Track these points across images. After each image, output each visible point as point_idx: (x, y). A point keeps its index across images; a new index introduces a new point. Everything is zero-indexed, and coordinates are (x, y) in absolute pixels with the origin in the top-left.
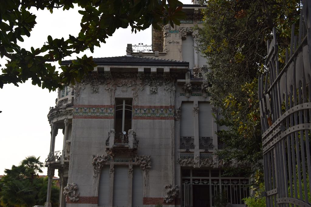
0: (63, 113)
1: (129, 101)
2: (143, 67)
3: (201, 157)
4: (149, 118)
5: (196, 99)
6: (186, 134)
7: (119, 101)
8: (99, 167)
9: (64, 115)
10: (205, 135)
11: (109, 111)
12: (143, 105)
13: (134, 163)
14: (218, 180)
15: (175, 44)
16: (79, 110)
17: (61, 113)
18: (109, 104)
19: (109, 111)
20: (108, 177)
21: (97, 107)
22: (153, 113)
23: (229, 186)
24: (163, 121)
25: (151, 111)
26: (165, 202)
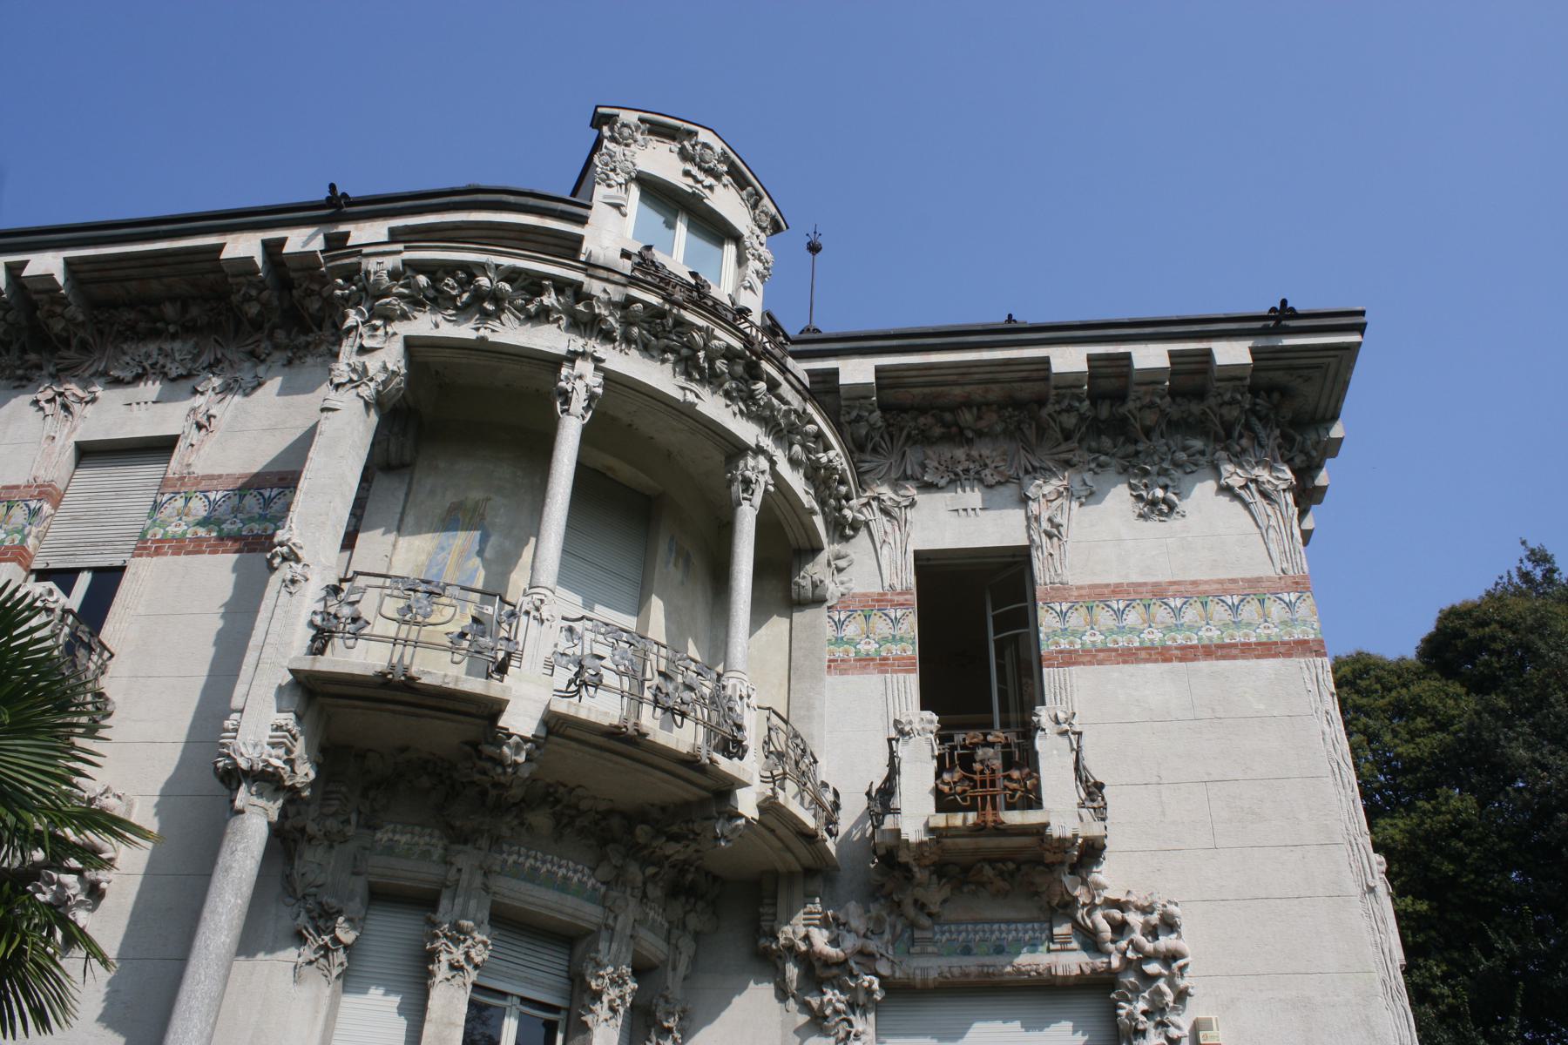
0: (775, 401)
17: (762, 386)
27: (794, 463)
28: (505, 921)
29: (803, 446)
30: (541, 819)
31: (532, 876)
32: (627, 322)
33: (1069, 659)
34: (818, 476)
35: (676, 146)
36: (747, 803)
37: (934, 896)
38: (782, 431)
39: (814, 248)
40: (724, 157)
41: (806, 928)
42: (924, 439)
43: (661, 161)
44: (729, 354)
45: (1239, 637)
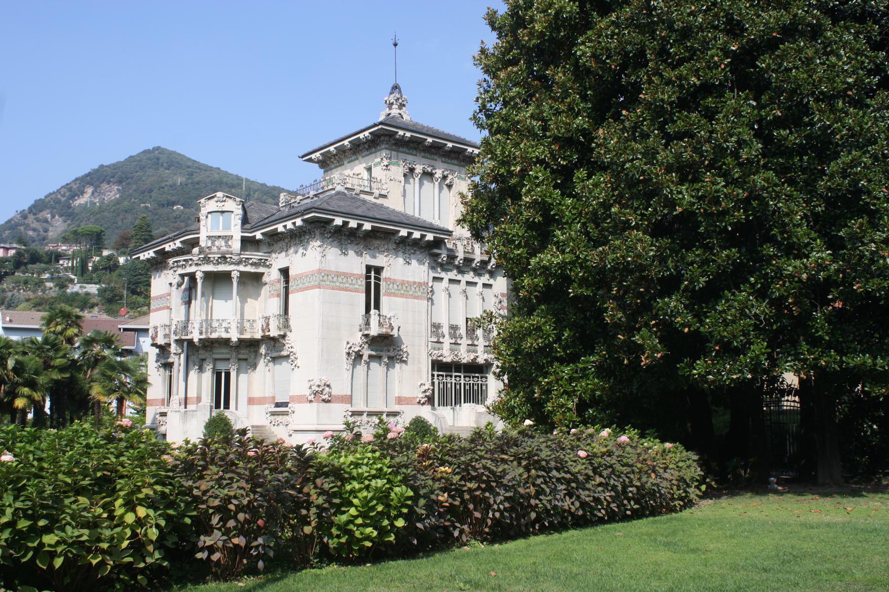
1: (378, 270)
2: (407, 230)
3: (452, 350)
4: (402, 296)
5: (446, 276)
6: (436, 320)
7: (369, 268)
9: (232, 263)
10: (454, 323)
11: (359, 282)
14: (460, 377)
16: (325, 278)
19: (359, 282)
20: (361, 369)
21: (346, 275)
22: (406, 289)
24: (416, 301)
25: (404, 288)
26: (419, 403)
27: (245, 266)
30: (216, 345)
34: (253, 264)
36: (234, 339)
37: (272, 343)
38: (239, 263)
39: (395, 45)
41: (263, 350)
42: (277, 241)
45: (310, 285)
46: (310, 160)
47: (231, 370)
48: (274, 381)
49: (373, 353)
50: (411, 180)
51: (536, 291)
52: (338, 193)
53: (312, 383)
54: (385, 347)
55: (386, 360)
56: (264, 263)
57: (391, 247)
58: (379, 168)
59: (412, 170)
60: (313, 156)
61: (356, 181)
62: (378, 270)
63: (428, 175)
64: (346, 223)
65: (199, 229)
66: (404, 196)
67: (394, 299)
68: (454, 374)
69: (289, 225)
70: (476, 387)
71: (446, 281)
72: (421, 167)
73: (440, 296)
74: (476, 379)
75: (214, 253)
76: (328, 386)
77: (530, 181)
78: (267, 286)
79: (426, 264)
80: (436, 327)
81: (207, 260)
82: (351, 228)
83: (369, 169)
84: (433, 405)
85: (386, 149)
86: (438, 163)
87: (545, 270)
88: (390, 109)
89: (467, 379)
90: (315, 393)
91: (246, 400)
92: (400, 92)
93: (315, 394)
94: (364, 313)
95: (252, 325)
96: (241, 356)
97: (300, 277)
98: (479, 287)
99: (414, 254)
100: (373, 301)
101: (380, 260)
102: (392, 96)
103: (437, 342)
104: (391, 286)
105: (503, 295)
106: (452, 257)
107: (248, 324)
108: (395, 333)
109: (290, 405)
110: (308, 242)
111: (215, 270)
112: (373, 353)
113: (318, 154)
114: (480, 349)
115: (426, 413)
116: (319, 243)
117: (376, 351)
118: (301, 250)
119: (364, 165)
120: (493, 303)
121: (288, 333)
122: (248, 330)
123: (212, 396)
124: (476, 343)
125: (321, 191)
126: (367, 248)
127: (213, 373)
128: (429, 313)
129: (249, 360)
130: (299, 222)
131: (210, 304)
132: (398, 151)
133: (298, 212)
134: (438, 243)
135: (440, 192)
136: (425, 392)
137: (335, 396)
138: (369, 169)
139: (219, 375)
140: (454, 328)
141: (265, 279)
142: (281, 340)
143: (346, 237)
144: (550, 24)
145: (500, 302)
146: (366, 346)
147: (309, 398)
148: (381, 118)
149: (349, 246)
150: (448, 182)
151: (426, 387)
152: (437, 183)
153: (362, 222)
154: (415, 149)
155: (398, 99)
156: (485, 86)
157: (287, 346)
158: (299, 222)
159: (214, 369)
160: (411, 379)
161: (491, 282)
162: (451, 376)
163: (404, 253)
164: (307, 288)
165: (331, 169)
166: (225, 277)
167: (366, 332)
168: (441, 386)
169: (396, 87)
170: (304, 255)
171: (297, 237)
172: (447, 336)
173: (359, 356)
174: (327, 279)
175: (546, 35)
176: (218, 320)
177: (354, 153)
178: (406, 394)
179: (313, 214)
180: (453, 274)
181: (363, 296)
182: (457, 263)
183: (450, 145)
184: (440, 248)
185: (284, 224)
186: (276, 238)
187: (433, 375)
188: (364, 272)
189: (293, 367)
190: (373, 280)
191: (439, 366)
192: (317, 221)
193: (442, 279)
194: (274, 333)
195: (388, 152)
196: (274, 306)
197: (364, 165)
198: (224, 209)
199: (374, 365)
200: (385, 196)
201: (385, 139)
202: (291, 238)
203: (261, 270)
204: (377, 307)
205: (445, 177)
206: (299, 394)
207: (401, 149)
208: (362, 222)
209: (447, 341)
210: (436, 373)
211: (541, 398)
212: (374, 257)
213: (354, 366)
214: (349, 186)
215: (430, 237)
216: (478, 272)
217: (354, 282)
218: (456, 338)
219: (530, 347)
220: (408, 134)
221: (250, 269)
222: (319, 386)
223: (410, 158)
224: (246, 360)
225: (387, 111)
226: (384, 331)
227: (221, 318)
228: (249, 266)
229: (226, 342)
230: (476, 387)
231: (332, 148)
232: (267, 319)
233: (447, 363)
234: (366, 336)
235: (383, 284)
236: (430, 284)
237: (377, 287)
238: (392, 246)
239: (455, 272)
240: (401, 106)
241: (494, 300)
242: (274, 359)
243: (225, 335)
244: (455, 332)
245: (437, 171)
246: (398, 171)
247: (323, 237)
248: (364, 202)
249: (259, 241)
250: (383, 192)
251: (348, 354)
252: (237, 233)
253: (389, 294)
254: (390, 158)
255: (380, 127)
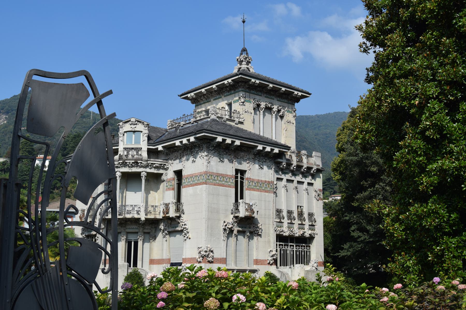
1: (243, 172)
2: (262, 146)
4: (258, 190)
6: (279, 208)
7: (237, 171)
8: (227, 232)
9: (142, 167)
11: (231, 181)
12: (254, 178)
13: (250, 229)
14: (293, 246)
15: (249, 114)
16: (210, 177)
17: (140, 164)
18: (231, 174)
19: (231, 181)
21: (223, 176)
22: (261, 186)
23: (284, 250)
24: (267, 194)
26: (269, 263)
28: (128, 233)
29: (150, 166)
30: (129, 223)
31: (130, 229)
32: (121, 165)
33: (185, 187)
34: (156, 168)
35: (128, 123)
36: (143, 219)
37: (169, 222)
39: (244, 22)
40: (136, 121)
41: (162, 227)
42: (173, 152)
43: (127, 127)
44: (133, 163)
46: (187, 98)
47: (139, 240)
48: (169, 248)
49: (240, 229)
50: (258, 112)
51: (431, 186)
52: (213, 120)
53: (201, 249)
54: (247, 226)
55: (248, 234)
56: (163, 167)
57: (251, 157)
58: (237, 104)
59: (259, 106)
60: (189, 95)
61: (223, 113)
62: (243, 172)
63: (269, 109)
64: (224, 140)
65: (118, 143)
66: (254, 123)
67: (253, 192)
68: (290, 244)
69: (185, 141)
70: (303, 253)
71: (285, 180)
72: (265, 104)
73: (282, 192)
74: (303, 248)
75: (130, 160)
76: (212, 251)
77: (429, 111)
78: (165, 183)
79: (273, 169)
80: (279, 212)
81: (124, 164)
82: (228, 144)
83: (230, 105)
84: (277, 266)
85: (242, 91)
86: (275, 101)
87: (442, 172)
88: (241, 64)
89: (298, 247)
90: (203, 257)
91: (148, 261)
92: (247, 54)
93: (203, 257)
94: (234, 202)
95: (155, 209)
96: (146, 231)
97: (191, 176)
98: (305, 186)
99: (265, 162)
100: (239, 194)
101: (244, 166)
102: (242, 56)
103: (279, 222)
104: (251, 183)
105: (320, 190)
106: (289, 164)
107: (152, 209)
108: (255, 215)
109: (183, 265)
110: (197, 153)
111: (130, 171)
112: (240, 229)
113: (192, 94)
114: (307, 227)
115: (273, 270)
116: (206, 154)
117: (242, 228)
118: (191, 159)
119: (226, 102)
120: (314, 196)
121: (182, 215)
122: (153, 213)
123: (125, 258)
124: (304, 223)
125: (198, 119)
126: (236, 157)
127: (126, 242)
128: (275, 202)
129: (151, 233)
130: (192, 139)
131: (124, 195)
132: (250, 93)
133: (193, 132)
134: (281, 155)
135: (276, 121)
136: (273, 256)
137: (216, 259)
138: (230, 105)
139: (129, 244)
140: (290, 213)
141: (163, 177)
142: (177, 220)
143: (223, 151)
144: (439, 5)
145: (319, 195)
146: (236, 225)
147: (199, 260)
148: (236, 71)
149: (225, 156)
150: (281, 114)
151: (274, 252)
152: (274, 115)
153: (234, 140)
154: (261, 91)
155: (246, 58)
156: (364, 47)
157: (181, 224)
158: (192, 139)
159: (126, 239)
160: (264, 247)
161: (313, 181)
162: (288, 246)
163: (259, 161)
164: (197, 184)
165: (201, 104)
166: (138, 175)
167: (236, 215)
168: (282, 252)
169: (244, 50)
170: (194, 161)
171: (189, 150)
172: (286, 218)
173: (231, 231)
174: (210, 178)
175: (435, 12)
176: (132, 206)
177: (219, 94)
178: (261, 257)
179: (203, 134)
180: (289, 176)
181: (233, 190)
182: (292, 168)
183: (283, 89)
184: (282, 158)
185: (180, 140)
186: (172, 150)
187: (277, 245)
188: (234, 174)
189: (185, 238)
190: (239, 179)
191: (280, 238)
192: (205, 139)
193: (282, 179)
194: (172, 214)
195: (244, 93)
196: (170, 197)
197: (226, 102)
198: (136, 129)
199: (240, 237)
200: (242, 123)
201: (244, 84)
202: (185, 150)
203: (161, 171)
204: (242, 198)
205: (279, 111)
206: (190, 257)
207: (252, 91)
208: (234, 140)
209: (286, 221)
210: (278, 243)
211: (433, 261)
212: (240, 163)
213: (228, 239)
214: (219, 115)
215: (276, 150)
216: (305, 175)
217: (228, 180)
218: (291, 219)
219: (430, 225)
220: (258, 82)
221: (153, 171)
222: (206, 252)
223: (258, 97)
224: (149, 233)
225: (239, 66)
226: (247, 214)
227: (134, 204)
228: (153, 169)
229: (136, 221)
230: (303, 253)
231: (203, 90)
232: (167, 205)
233: (286, 237)
234: (236, 217)
235: (246, 183)
236: (275, 183)
237: (242, 183)
238: (251, 156)
239: (290, 174)
240: (248, 63)
241: (314, 193)
242: (170, 233)
243: (136, 216)
244: (290, 216)
245: (274, 106)
246: (250, 106)
247: (208, 150)
248: (231, 126)
249: (161, 151)
250: (241, 120)
251: (225, 230)
252: (144, 146)
253: (249, 189)
254: (245, 97)
255: (240, 76)
